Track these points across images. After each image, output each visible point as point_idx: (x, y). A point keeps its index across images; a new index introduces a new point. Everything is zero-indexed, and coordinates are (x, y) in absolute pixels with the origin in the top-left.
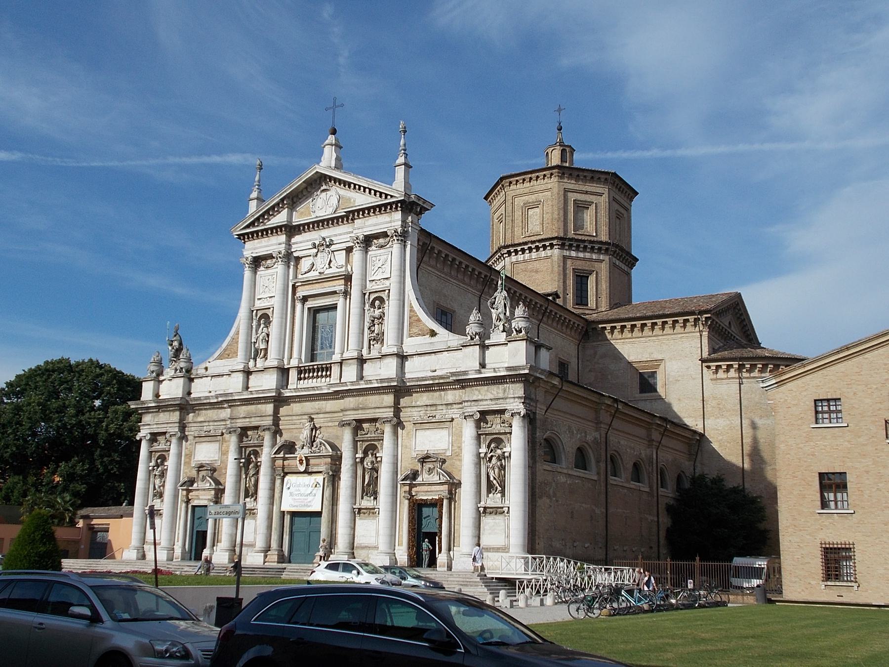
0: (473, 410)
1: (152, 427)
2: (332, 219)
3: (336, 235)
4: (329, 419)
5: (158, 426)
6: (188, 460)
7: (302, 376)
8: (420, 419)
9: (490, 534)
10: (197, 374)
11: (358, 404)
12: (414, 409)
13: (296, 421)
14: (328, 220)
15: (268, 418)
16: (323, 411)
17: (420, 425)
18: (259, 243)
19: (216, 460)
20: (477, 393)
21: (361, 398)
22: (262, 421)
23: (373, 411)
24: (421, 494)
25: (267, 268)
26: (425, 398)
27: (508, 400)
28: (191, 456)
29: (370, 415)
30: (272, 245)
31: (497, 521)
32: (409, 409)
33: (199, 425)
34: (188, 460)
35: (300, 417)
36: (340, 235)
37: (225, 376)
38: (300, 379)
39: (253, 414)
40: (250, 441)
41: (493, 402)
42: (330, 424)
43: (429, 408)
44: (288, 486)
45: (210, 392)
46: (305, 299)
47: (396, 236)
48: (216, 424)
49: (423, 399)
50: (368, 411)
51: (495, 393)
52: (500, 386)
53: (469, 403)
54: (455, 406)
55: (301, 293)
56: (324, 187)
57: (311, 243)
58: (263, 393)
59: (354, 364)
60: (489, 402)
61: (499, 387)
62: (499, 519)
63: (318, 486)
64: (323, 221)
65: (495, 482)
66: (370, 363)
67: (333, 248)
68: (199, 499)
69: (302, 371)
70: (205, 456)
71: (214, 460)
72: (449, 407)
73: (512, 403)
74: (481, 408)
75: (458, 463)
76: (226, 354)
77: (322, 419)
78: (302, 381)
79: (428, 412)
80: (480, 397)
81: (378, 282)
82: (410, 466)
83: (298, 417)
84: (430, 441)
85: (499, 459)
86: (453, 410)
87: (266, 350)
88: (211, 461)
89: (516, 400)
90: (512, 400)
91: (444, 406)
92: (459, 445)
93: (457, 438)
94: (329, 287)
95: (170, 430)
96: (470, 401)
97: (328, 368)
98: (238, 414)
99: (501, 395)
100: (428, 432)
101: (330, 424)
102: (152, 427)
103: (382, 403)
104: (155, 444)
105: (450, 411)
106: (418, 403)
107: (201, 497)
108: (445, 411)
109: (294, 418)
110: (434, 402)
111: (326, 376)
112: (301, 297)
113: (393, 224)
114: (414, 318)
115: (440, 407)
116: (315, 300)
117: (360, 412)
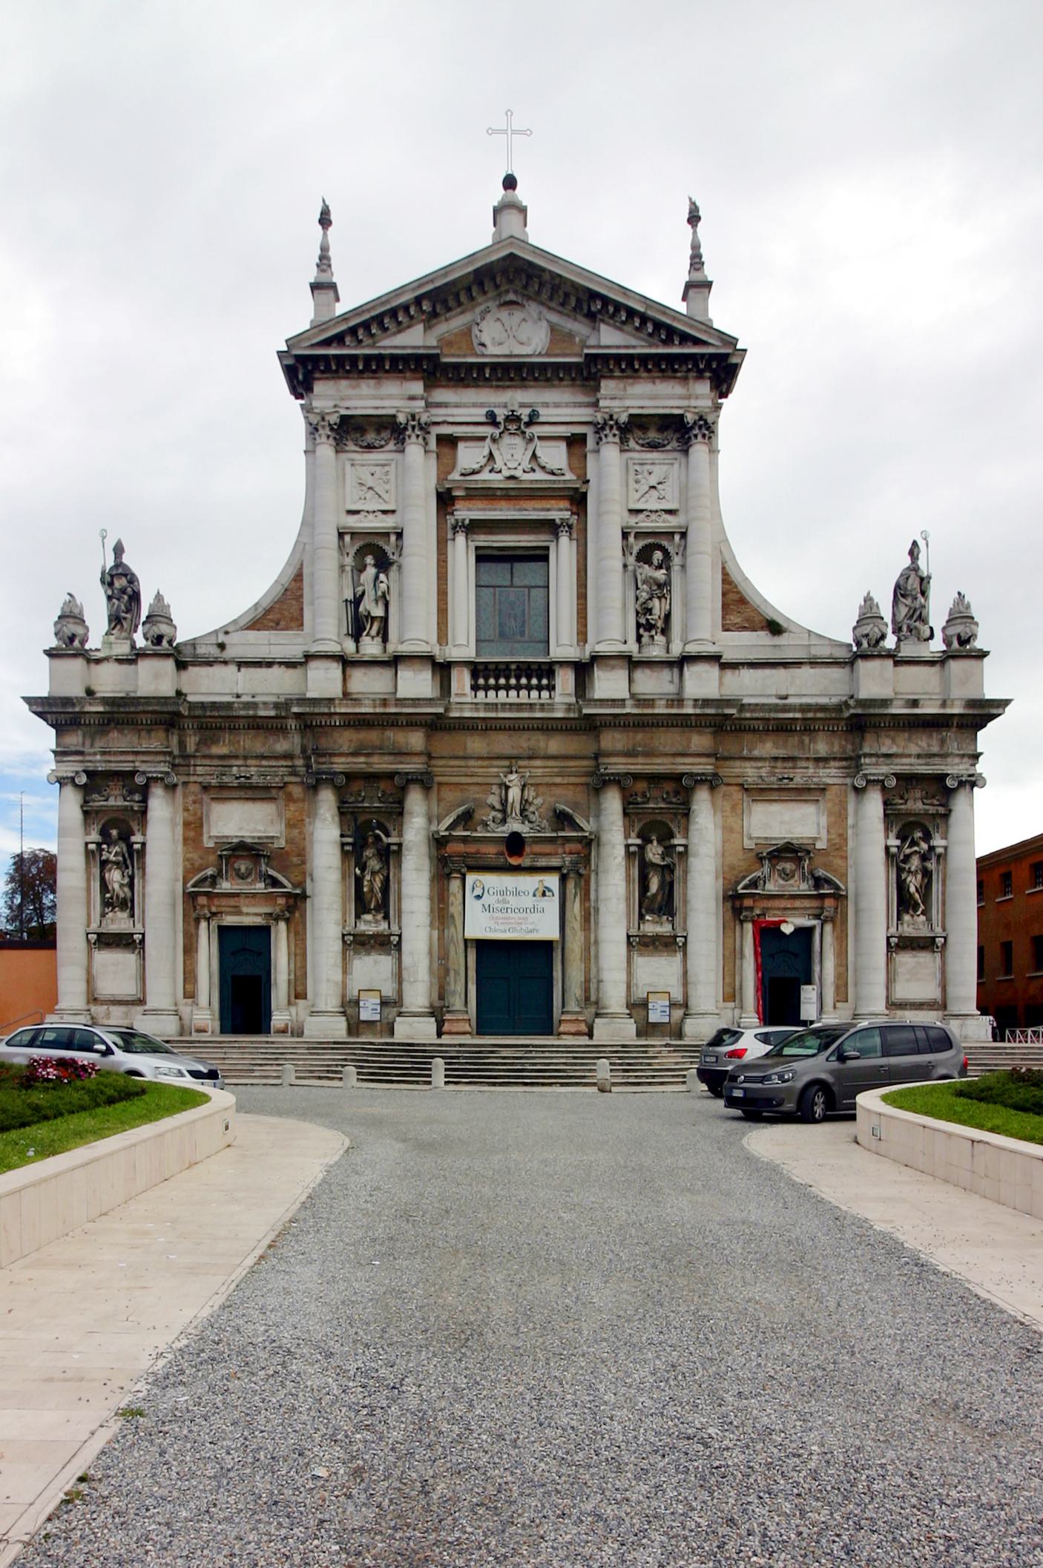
0: (880, 771)
1: (88, 758)
2: (544, 366)
3: (546, 405)
4: (556, 770)
5: (108, 758)
6: (191, 834)
7: (481, 681)
8: (760, 781)
9: (908, 980)
10: (195, 656)
11: (634, 746)
12: (748, 764)
13: (476, 770)
14: (532, 366)
15: (416, 759)
16: (542, 753)
17: (760, 793)
18: (354, 388)
19: (272, 837)
20: (888, 742)
21: (639, 736)
22: (401, 763)
23: (666, 760)
24: (772, 912)
25: (366, 447)
26: (769, 745)
27: (949, 760)
28: (201, 826)
29: (661, 767)
30: (390, 397)
31: (922, 960)
32: (738, 763)
33: (216, 762)
34: (191, 834)
35: (485, 763)
36: (557, 405)
37: (276, 668)
38: (475, 688)
39: (374, 747)
40: (362, 801)
41: (921, 761)
42: (558, 780)
43: (779, 764)
44: (476, 893)
45: (238, 696)
46: (473, 527)
47: (700, 427)
48: (264, 763)
49: (768, 748)
50: (659, 761)
51: (924, 744)
52: (934, 735)
53: (874, 760)
54: (832, 763)
55: (465, 513)
56: (511, 297)
57: (484, 411)
58: (414, 706)
59: (622, 668)
60: (913, 760)
61: (931, 736)
62: (924, 958)
63: (547, 893)
64: (519, 367)
65: (917, 895)
66: (647, 672)
67: (537, 430)
68: (240, 913)
69: (500, 671)
70: (241, 829)
71: (267, 837)
72: (821, 764)
73: (958, 764)
74: (898, 769)
75: (839, 862)
76: (272, 621)
77: (541, 770)
78: (481, 694)
79: (777, 771)
80: (894, 750)
81: (653, 516)
82: (741, 864)
83: (480, 763)
84: (781, 822)
85: (924, 858)
86: (828, 771)
87: (385, 620)
88: (259, 838)
89: (966, 760)
90: (957, 760)
91: (810, 764)
92: (841, 831)
93: (839, 817)
94: (535, 509)
95: (143, 768)
96: (877, 756)
97: (546, 671)
98: (336, 747)
99: (935, 749)
100: (776, 808)
101: (558, 780)
102: (88, 758)
103: (689, 747)
104: (95, 796)
105: (822, 771)
106: (756, 753)
107: (245, 910)
108: (812, 771)
109: (472, 763)
110: (796, 754)
111: (540, 688)
112: (467, 522)
113: (693, 403)
114: (731, 596)
115: (804, 764)
116: (491, 533)
117: (640, 760)
